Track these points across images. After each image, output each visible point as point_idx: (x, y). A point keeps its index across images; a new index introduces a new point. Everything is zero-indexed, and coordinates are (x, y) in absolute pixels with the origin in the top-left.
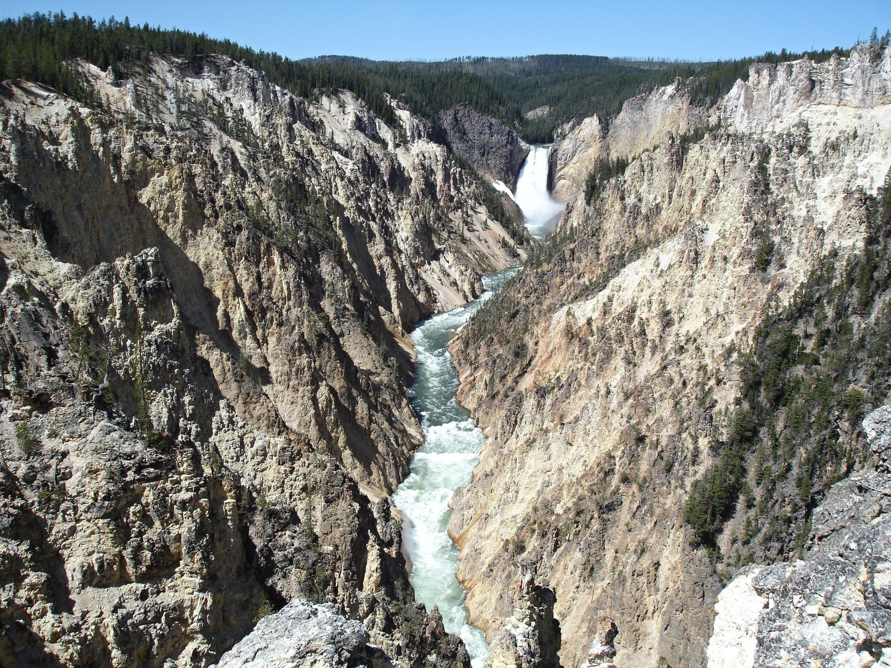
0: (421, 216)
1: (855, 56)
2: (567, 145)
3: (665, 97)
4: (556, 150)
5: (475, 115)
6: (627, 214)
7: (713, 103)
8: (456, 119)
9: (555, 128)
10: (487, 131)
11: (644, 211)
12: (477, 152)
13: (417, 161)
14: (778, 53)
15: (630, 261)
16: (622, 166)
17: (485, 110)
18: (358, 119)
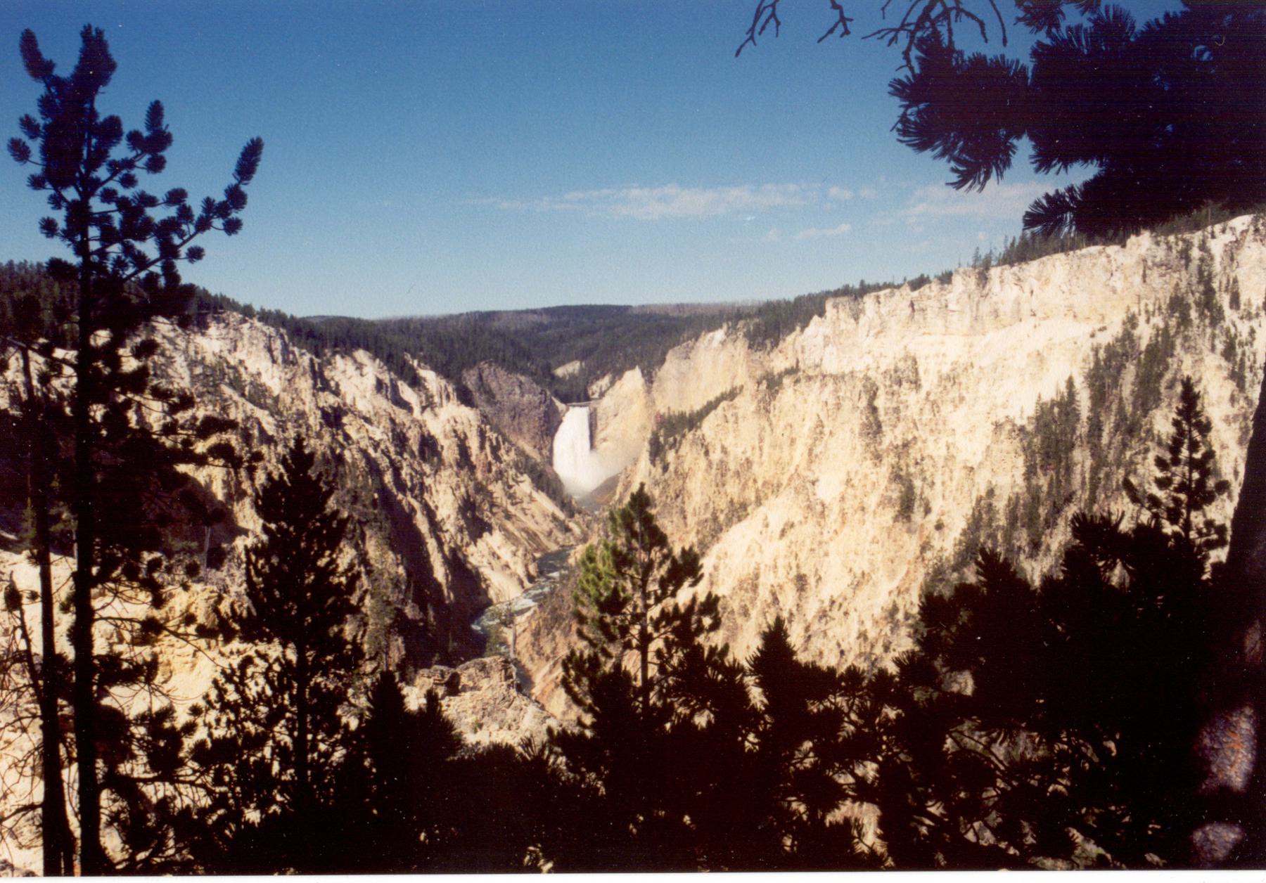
0: (463, 490)
1: (957, 279)
2: (607, 402)
3: (715, 344)
4: (595, 409)
5: (502, 373)
6: (714, 471)
7: (775, 344)
8: (481, 378)
9: (588, 383)
10: (517, 390)
11: (732, 466)
12: (507, 416)
13: (448, 428)
14: (857, 286)
15: (729, 522)
16: (692, 421)
17: (512, 368)
18: (380, 385)
